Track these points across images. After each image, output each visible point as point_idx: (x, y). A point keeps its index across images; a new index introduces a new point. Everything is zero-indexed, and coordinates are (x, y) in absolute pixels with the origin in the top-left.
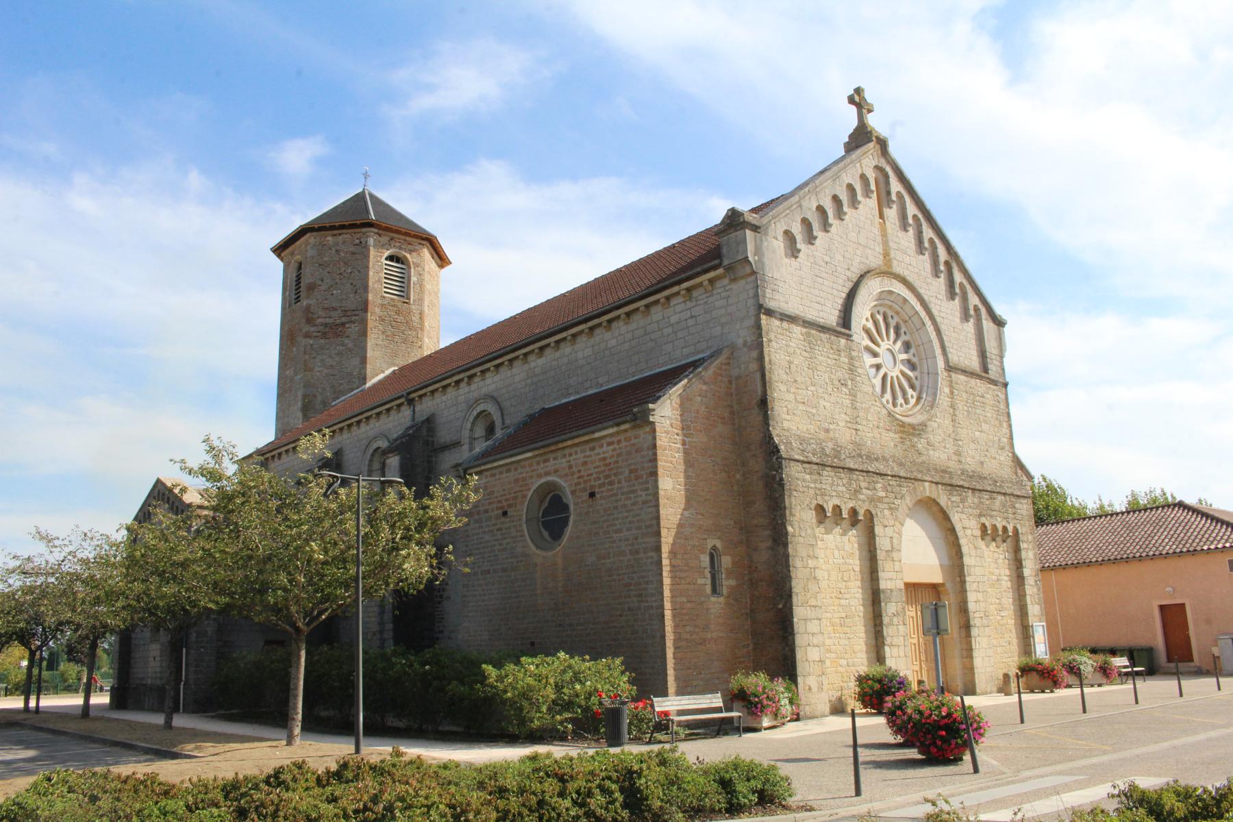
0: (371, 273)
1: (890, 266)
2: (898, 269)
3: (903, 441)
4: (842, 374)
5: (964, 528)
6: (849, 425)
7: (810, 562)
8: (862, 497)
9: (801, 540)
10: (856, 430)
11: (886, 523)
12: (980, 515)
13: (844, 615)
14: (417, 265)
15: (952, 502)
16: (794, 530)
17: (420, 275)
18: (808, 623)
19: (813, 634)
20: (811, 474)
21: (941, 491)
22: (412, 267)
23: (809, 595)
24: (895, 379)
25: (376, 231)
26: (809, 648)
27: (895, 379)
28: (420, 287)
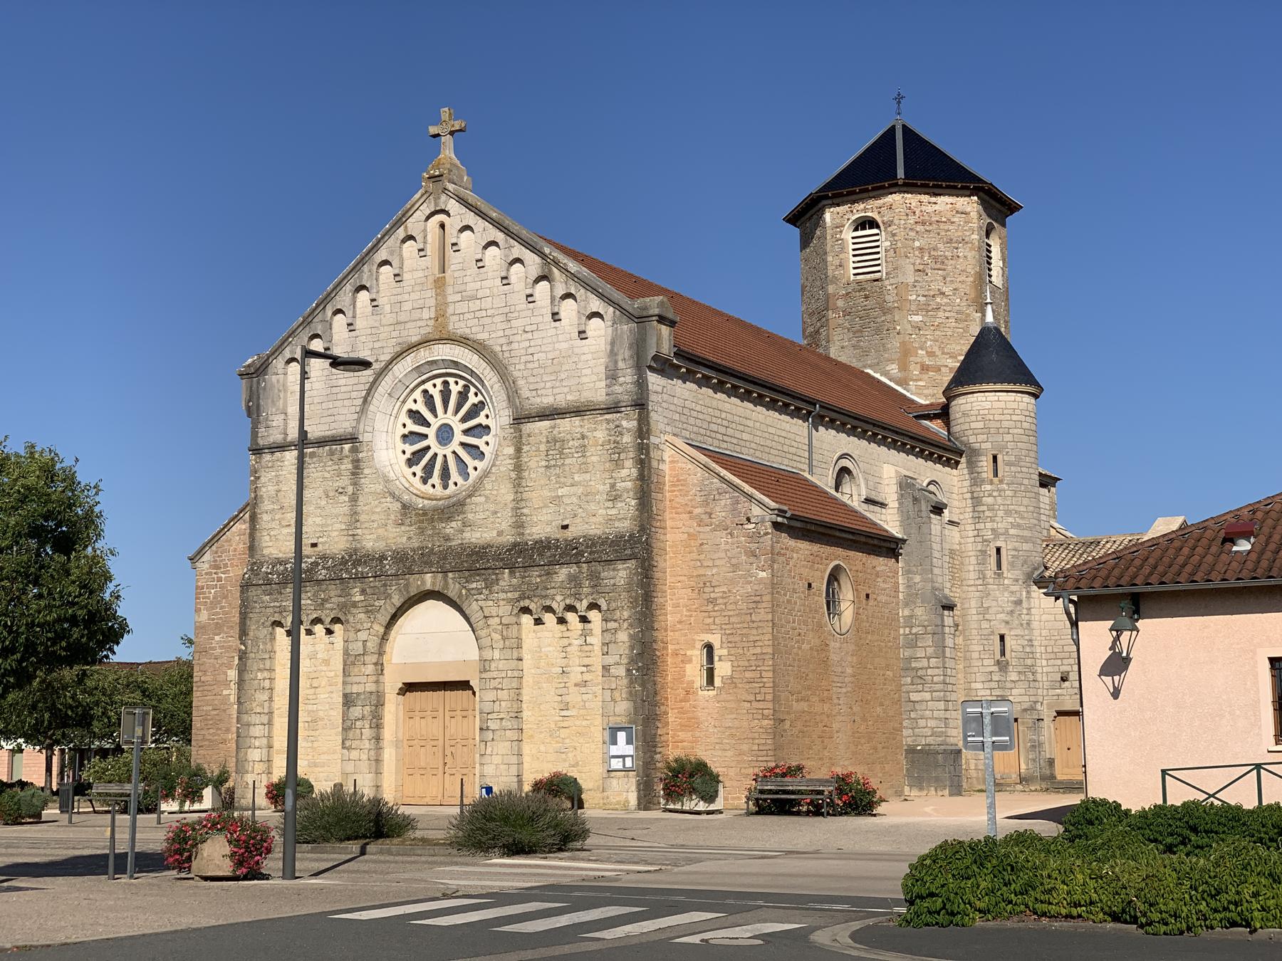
0: (830, 259)
1: (445, 326)
2: (457, 326)
3: (422, 531)
4: (345, 481)
5: (485, 617)
6: (346, 532)
7: (259, 674)
8: (328, 606)
9: (252, 655)
10: (354, 535)
11: (359, 626)
12: (522, 598)
13: (309, 719)
14: (889, 224)
15: (469, 590)
16: (246, 647)
17: (894, 235)
18: (251, 728)
19: (255, 738)
20: (270, 594)
21: (450, 581)
22: (882, 228)
23: (254, 705)
24: (439, 460)
25: (830, 202)
26: (250, 750)
27: (439, 460)
28: (895, 253)
